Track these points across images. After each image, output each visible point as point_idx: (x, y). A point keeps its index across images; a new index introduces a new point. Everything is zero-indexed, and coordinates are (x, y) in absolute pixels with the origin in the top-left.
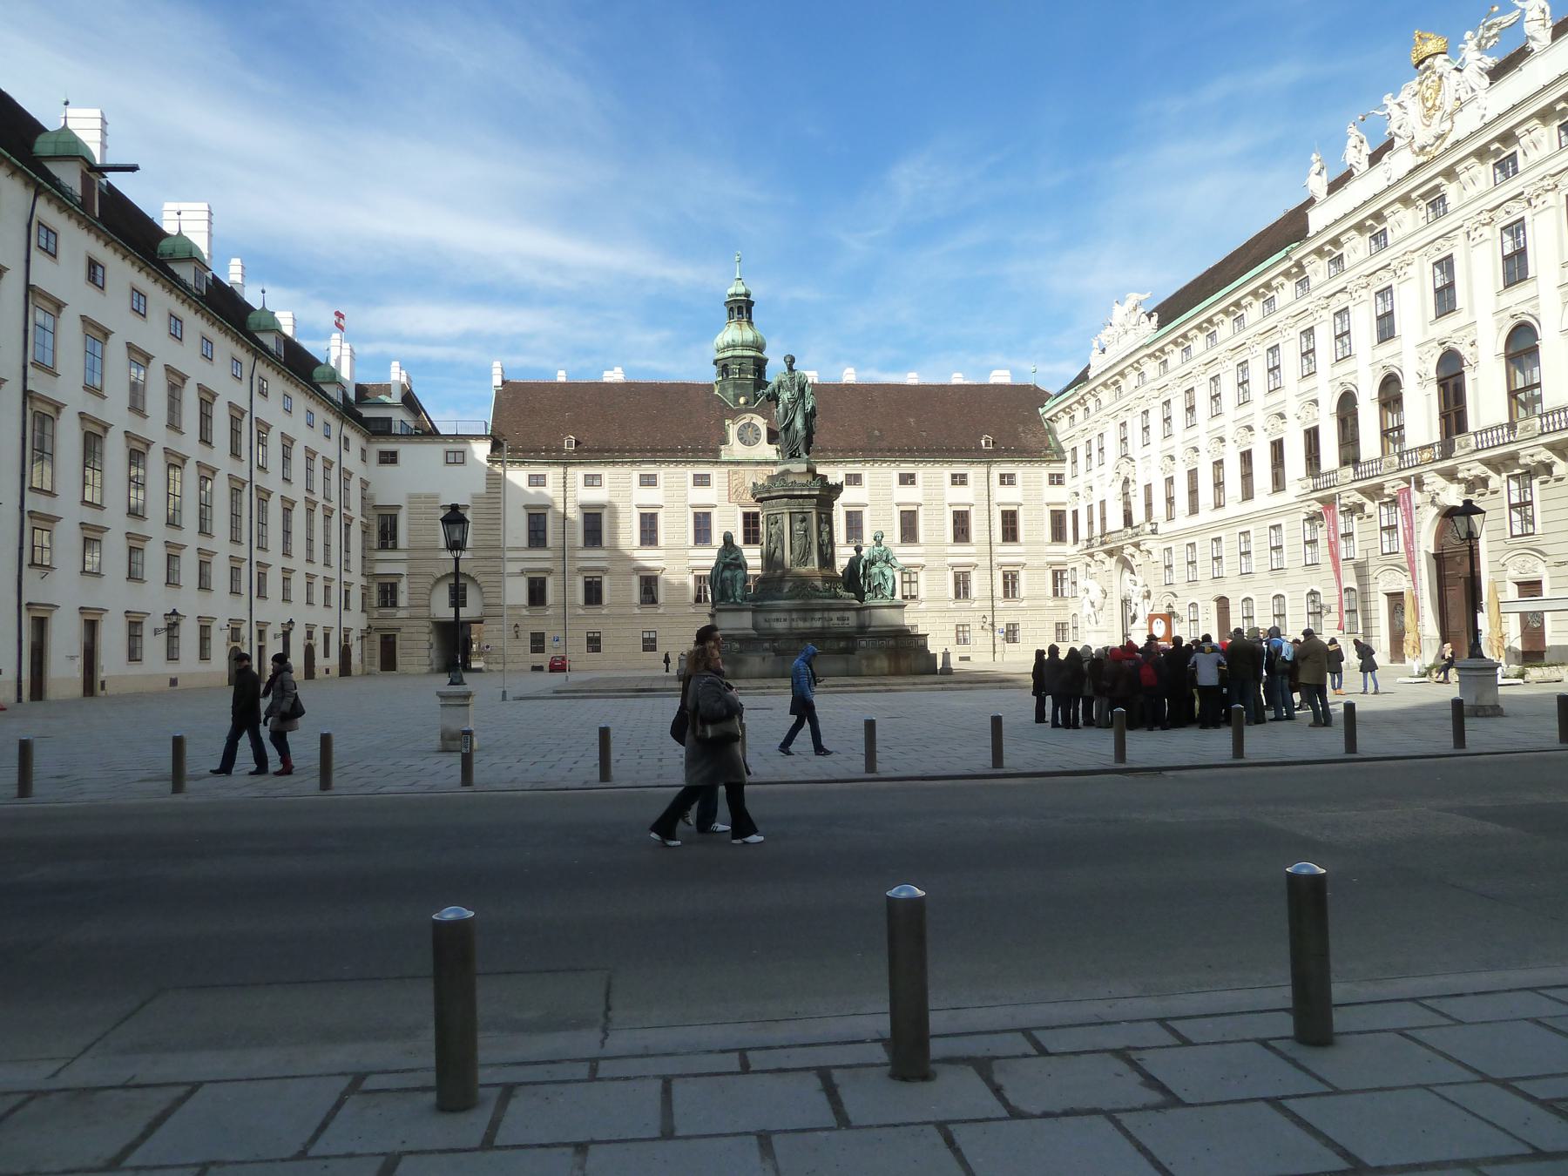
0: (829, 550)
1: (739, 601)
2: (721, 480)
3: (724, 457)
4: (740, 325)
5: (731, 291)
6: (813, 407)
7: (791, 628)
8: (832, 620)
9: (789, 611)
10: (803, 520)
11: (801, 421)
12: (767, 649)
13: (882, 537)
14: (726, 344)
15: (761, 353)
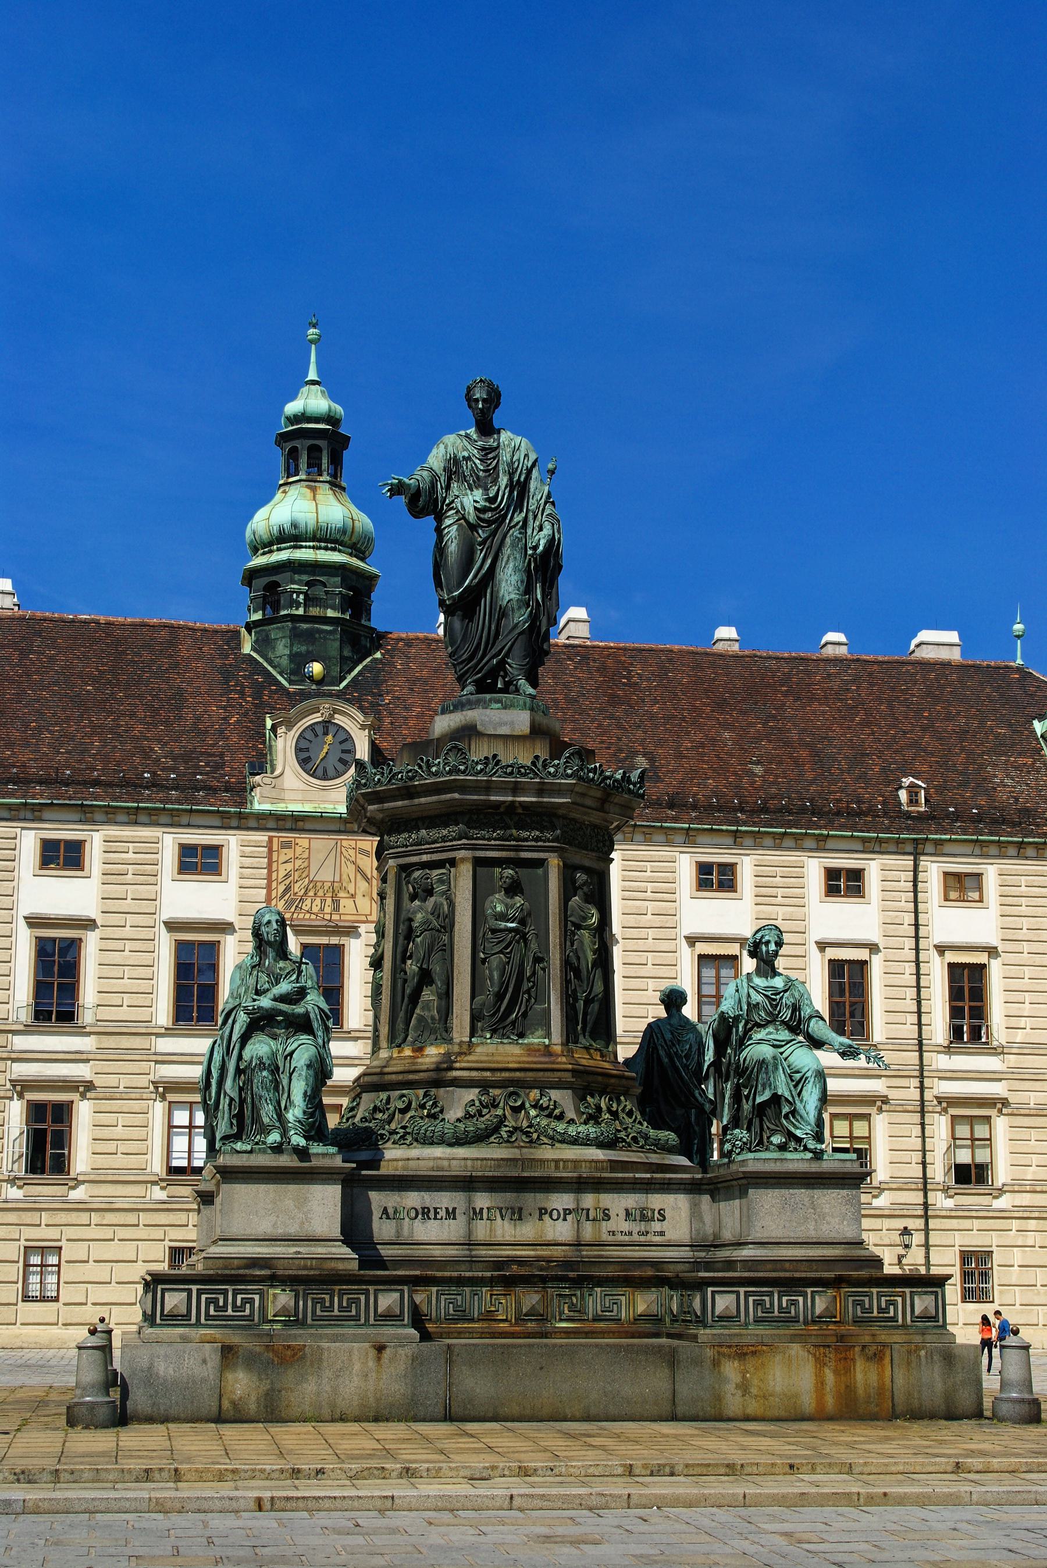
0: (599, 987)
1: (298, 1140)
2: (248, 861)
3: (259, 804)
4: (314, 490)
5: (293, 407)
6: (552, 543)
7: (470, 1244)
8: (607, 1217)
9: (467, 1184)
10: (513, 889)
11: (514, 579)
12: (388, 1317)
13: (779, 944)
14: (275, 532)
15: (363, 559)
